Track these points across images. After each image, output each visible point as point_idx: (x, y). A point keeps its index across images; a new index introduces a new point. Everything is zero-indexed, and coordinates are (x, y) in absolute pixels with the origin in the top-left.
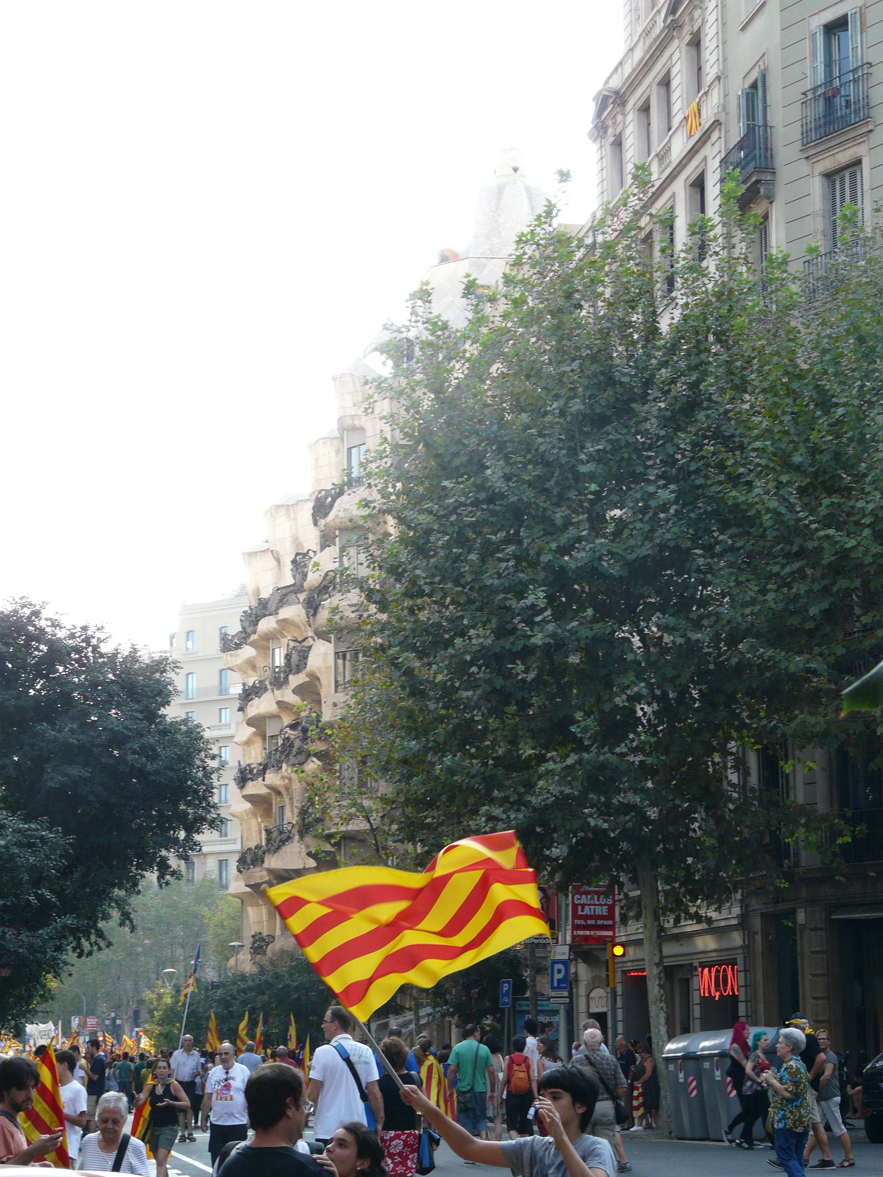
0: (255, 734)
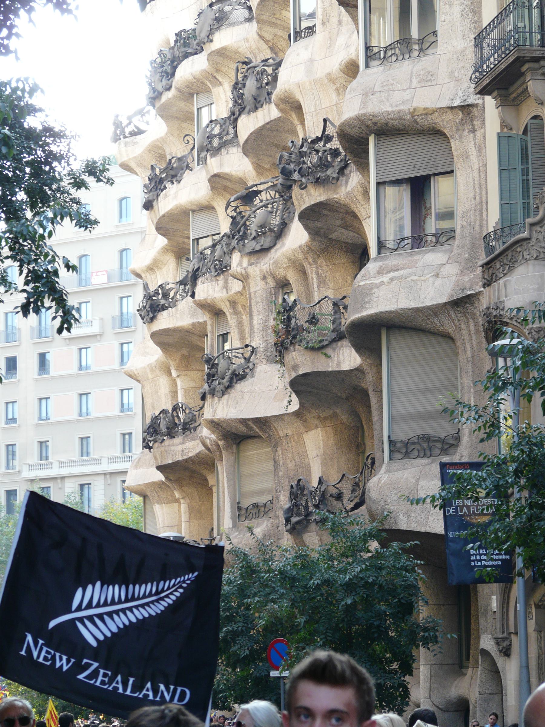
0: (165, 250)
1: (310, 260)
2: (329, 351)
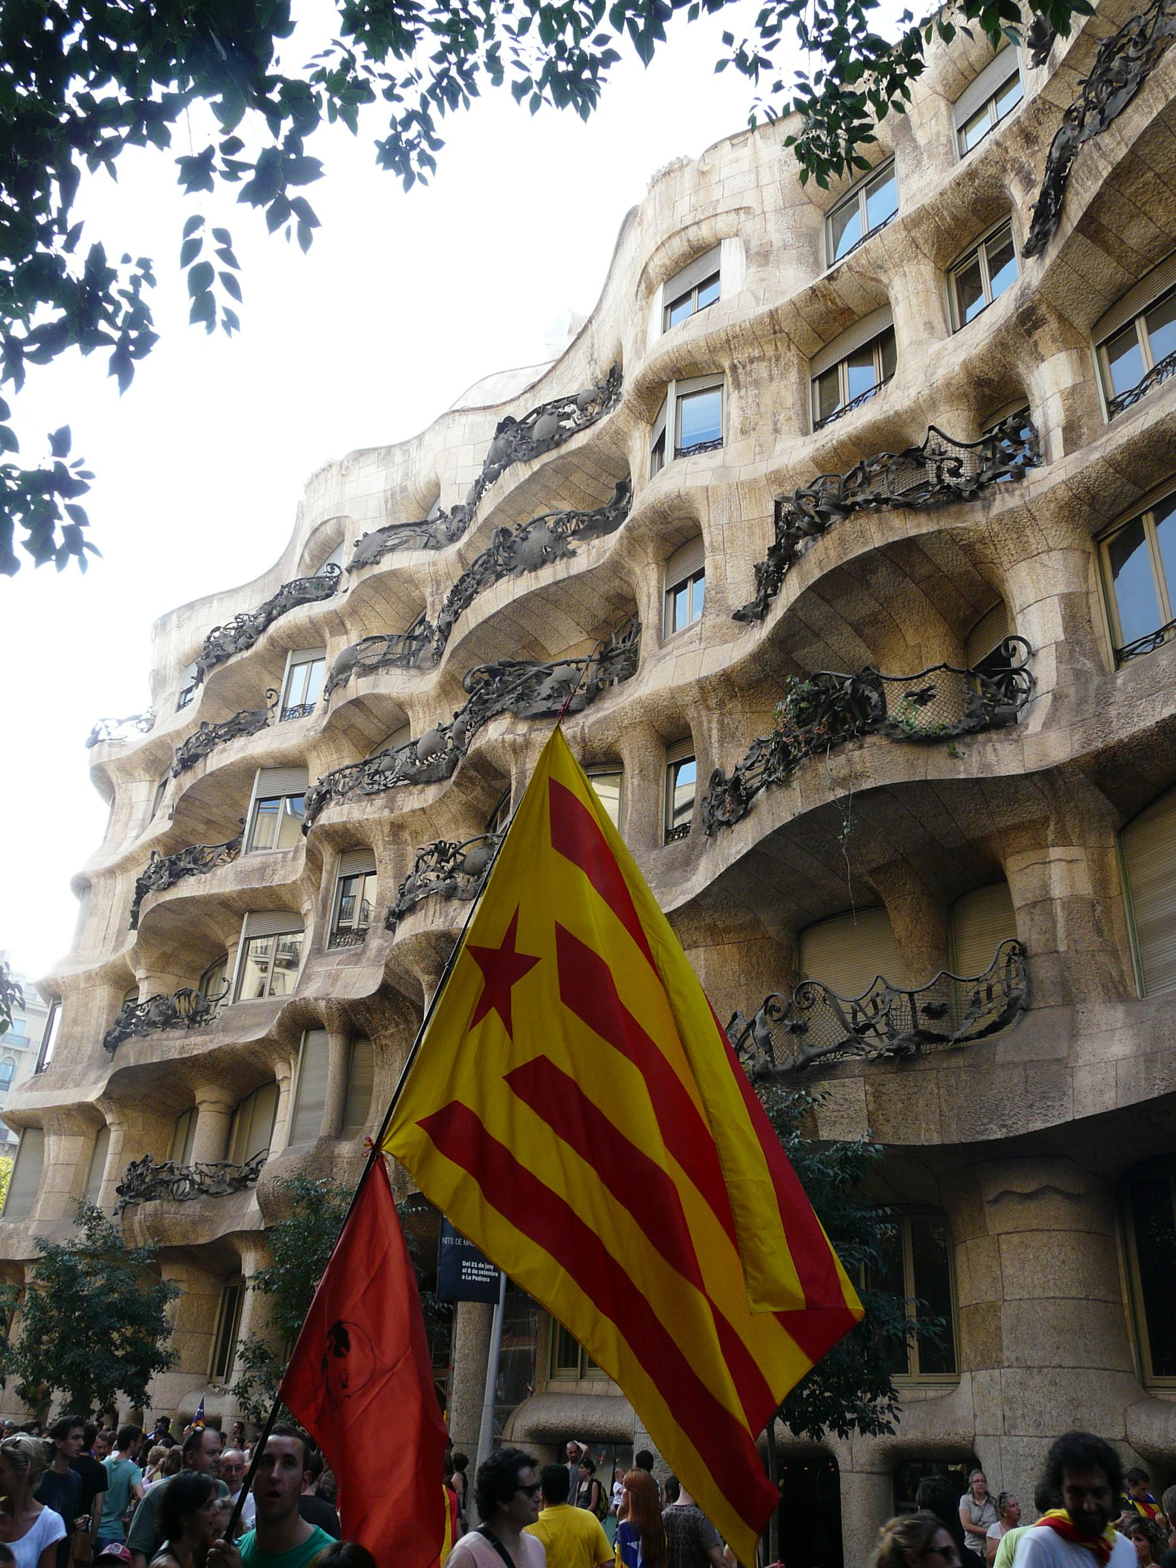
1: (712, 703)
2: (960, 749)
